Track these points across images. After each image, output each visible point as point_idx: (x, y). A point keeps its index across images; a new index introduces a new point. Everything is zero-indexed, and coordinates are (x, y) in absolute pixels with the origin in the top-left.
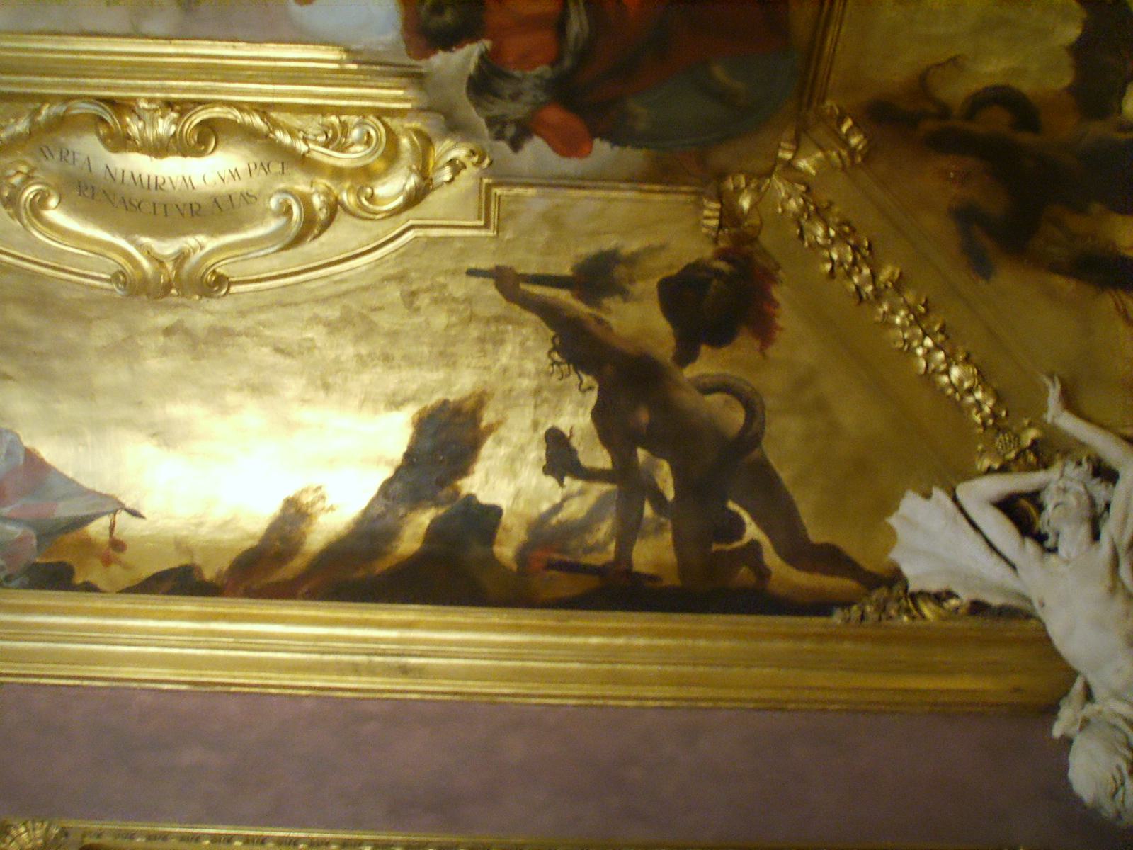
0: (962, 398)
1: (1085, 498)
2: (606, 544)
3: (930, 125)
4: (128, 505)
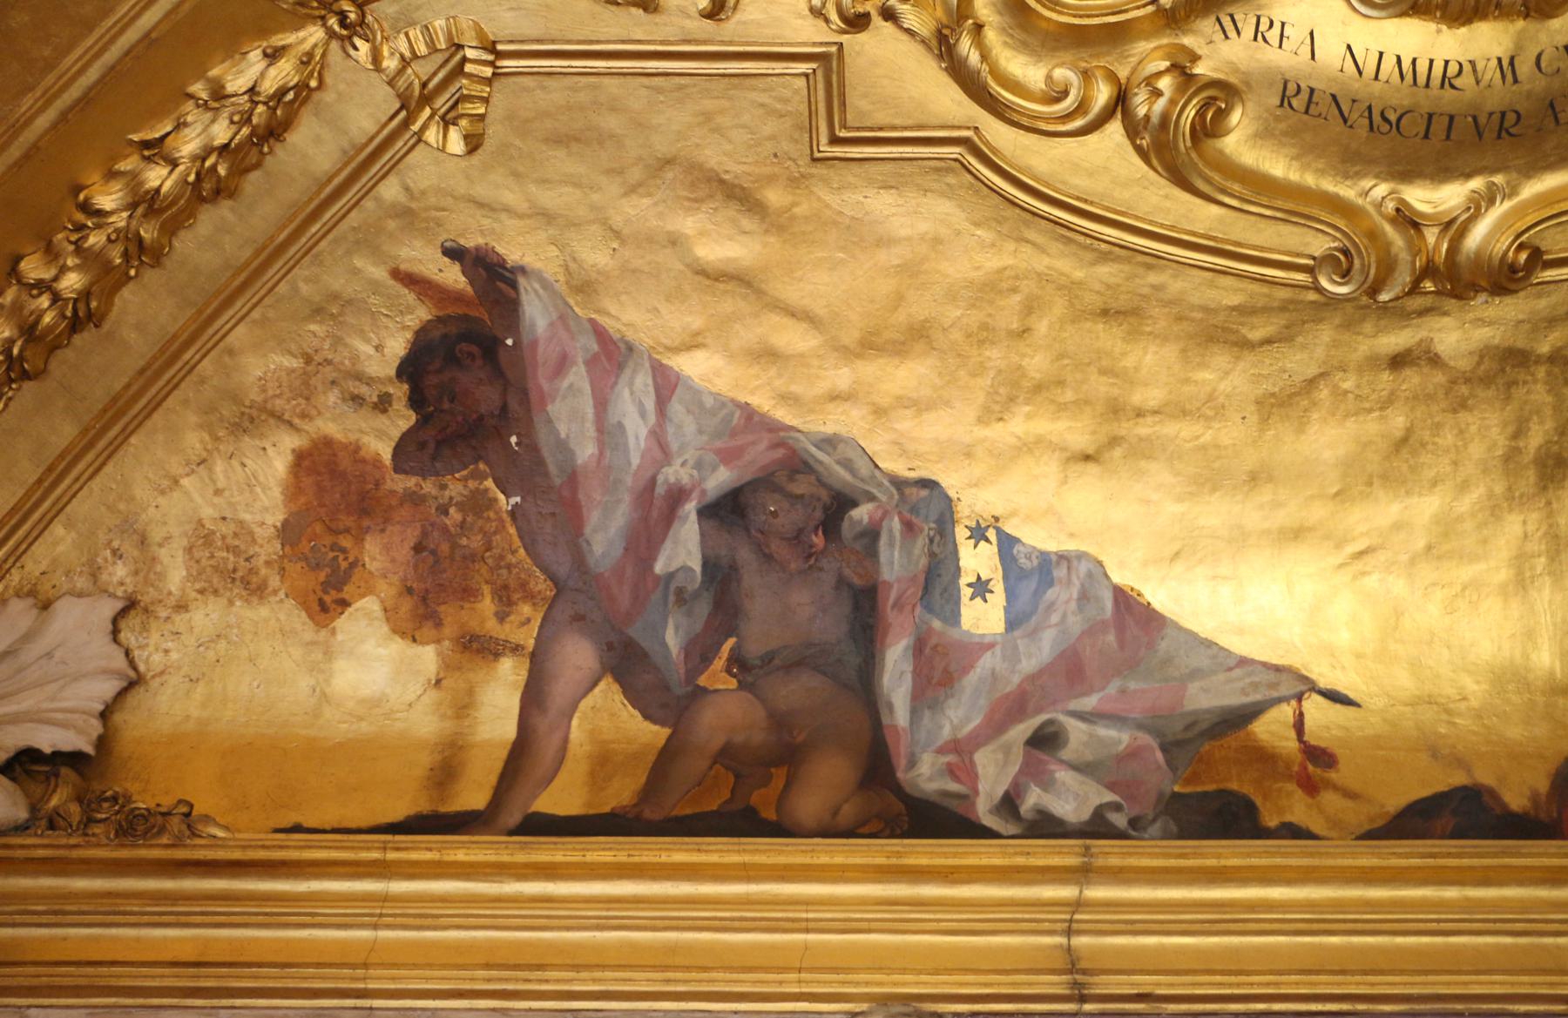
4: (1323, 683)
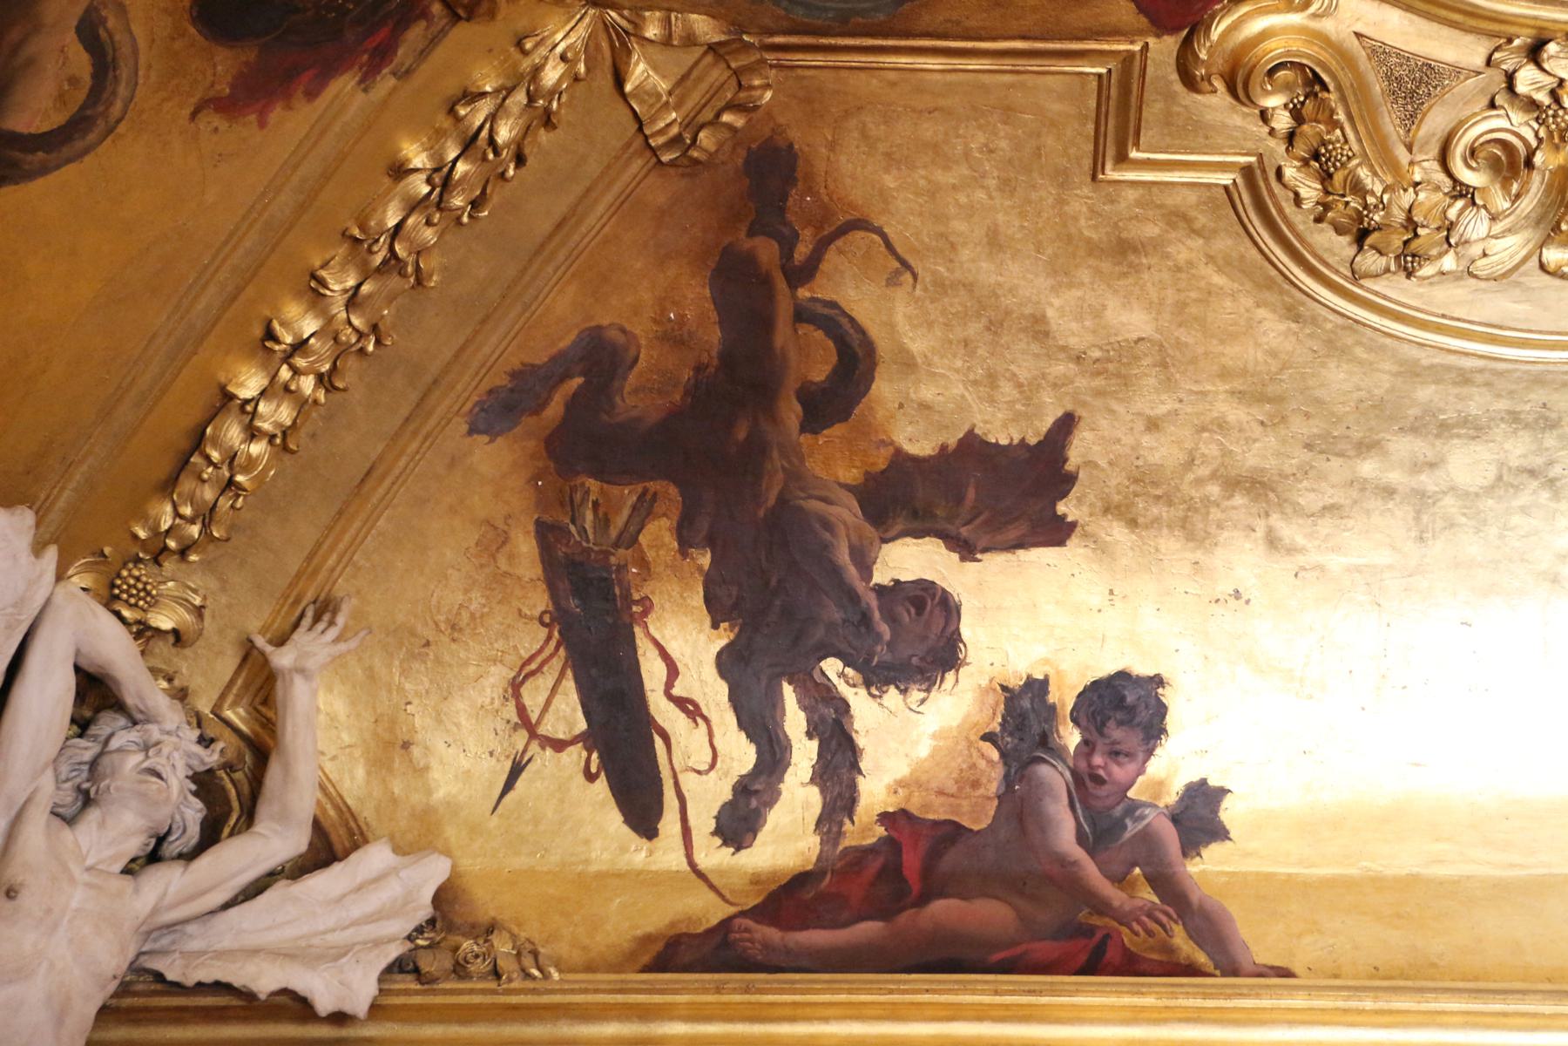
3: (767, 251)
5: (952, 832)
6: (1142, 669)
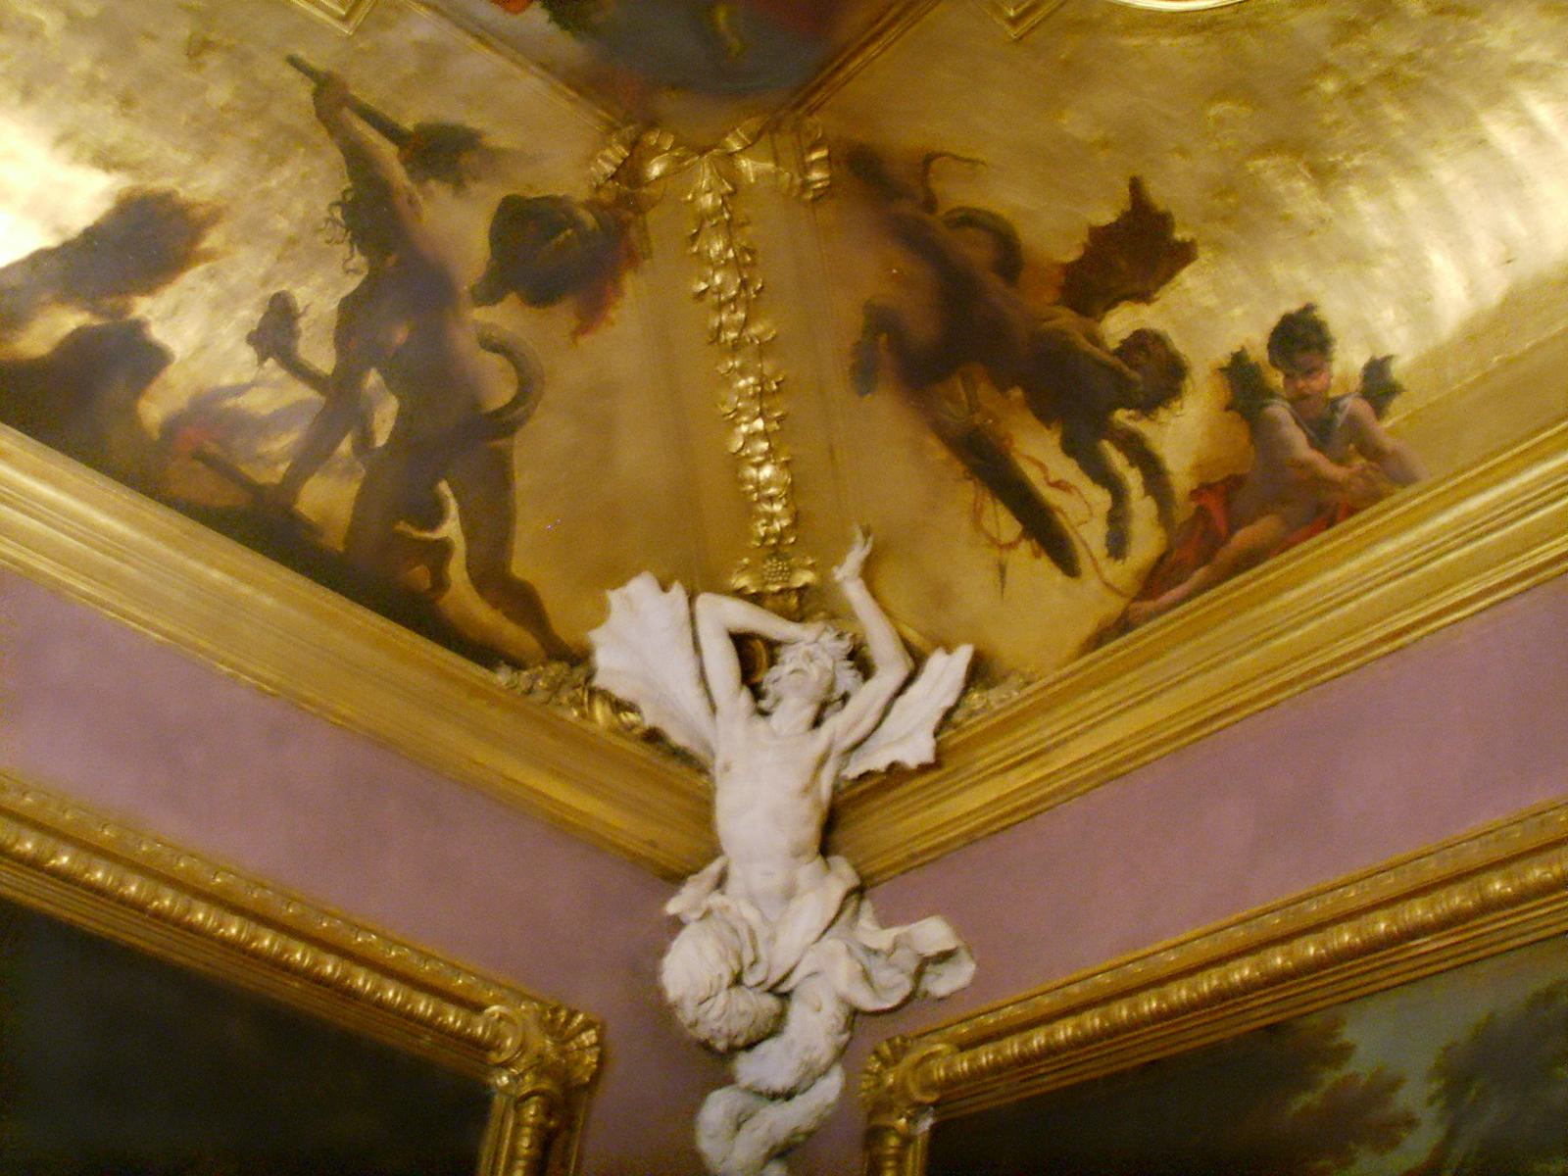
0: (759, 501)
1: (827, 678)
2: (276, 464)
3: (907, 208)
5: (1234, 483)
6: (1292, 306)
